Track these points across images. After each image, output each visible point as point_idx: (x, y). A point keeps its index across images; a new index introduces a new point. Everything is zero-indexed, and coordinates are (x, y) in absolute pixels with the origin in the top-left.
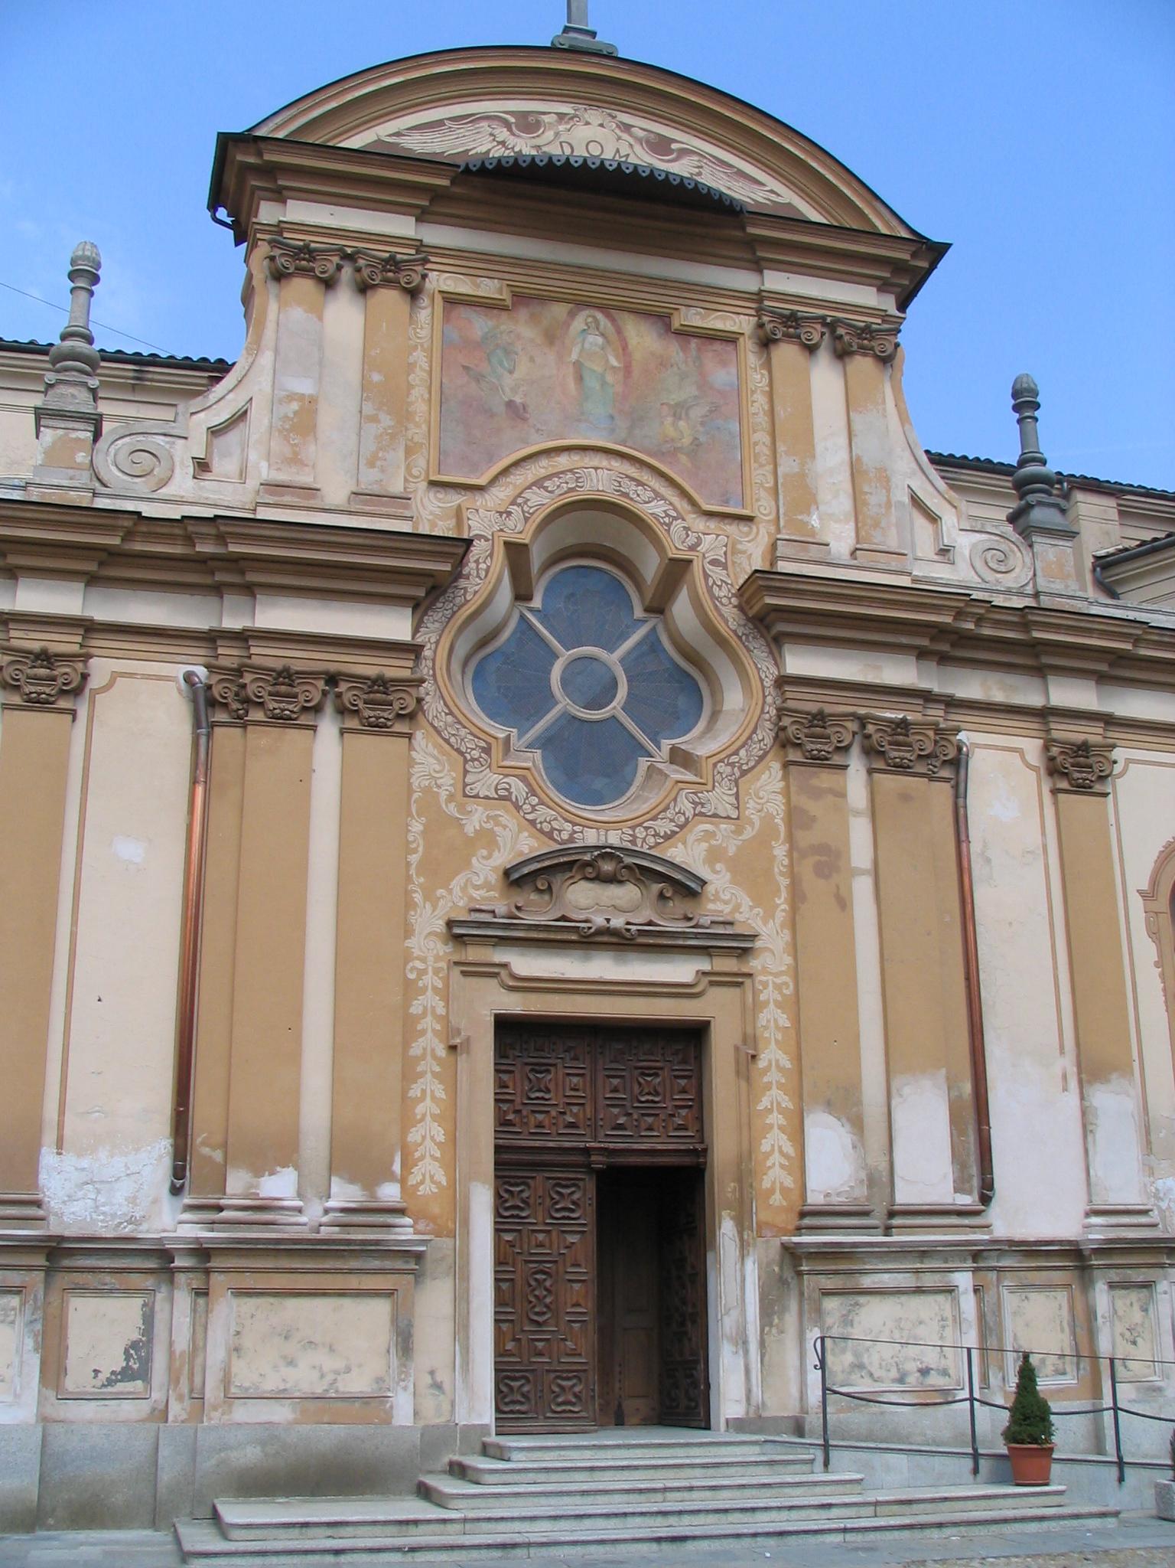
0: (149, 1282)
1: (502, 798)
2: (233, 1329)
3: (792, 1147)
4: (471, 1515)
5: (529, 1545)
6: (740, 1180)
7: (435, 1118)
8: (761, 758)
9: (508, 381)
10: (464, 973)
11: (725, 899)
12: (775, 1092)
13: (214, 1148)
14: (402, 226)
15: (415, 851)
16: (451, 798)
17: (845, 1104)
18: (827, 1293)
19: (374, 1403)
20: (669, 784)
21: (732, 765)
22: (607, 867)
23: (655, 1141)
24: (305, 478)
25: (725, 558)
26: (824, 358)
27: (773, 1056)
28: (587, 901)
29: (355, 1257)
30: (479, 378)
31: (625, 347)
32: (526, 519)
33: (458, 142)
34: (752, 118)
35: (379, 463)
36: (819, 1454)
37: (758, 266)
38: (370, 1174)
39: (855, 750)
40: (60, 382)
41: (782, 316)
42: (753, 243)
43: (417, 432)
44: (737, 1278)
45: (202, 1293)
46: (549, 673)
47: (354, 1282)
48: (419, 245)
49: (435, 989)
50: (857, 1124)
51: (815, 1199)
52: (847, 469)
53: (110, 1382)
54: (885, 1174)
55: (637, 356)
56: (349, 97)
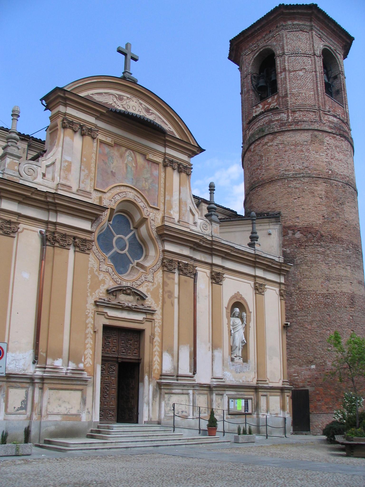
0: (27, 385)
1: (107, 272)
2: (48, 397)
3: (161, 360)
4: (117, 441)
5: (131, 447)
6: (149, 367)
7: (90, 348)
8: (158, 268)
9: (112, 166)
10: (98, 314)
11: (150, 302)
12: (157, 347)
13: (43, 353)
14: (92, 120)
15: (88, 283)
16: (97, 271)
17: (170, 351)
18: (166, 393)
19: (78, 416)
20: (140, 272)
21: (152, 269)
22: (129, 291)
23: (130, 356)
24: (68, 184)
25: (155, 219)
26: (176, 171)
27: (157, 339)
28: (123, 299)
29: (73, 381)
30: (106, 164)
31: (136, 161)
32: (115, 203)
33: (105, 100)
34: (168, 109)
35: (84, 182)
36: (172, 429)
37: (165, 146)
38: (78, 361)
39: (176, 269)
40: (12, 145)
41: (170, 160)
42: (166, 141)
43: (92, 175)
44: (147, 390)
45: (42, 389)
46: (112, 240)
47: (74, 387)
48: (96, 126)
49: (91, 317)
50: (172, 356)
51: (164, 372)
52: (178, 200)
53: (18, 410)
54: (177, 367)
55: (139, 164)
56: (85, 83)
